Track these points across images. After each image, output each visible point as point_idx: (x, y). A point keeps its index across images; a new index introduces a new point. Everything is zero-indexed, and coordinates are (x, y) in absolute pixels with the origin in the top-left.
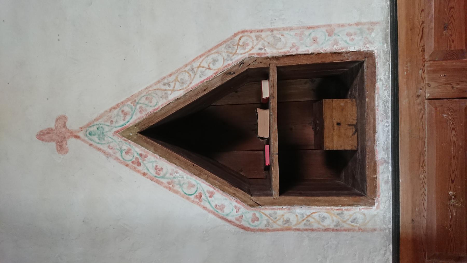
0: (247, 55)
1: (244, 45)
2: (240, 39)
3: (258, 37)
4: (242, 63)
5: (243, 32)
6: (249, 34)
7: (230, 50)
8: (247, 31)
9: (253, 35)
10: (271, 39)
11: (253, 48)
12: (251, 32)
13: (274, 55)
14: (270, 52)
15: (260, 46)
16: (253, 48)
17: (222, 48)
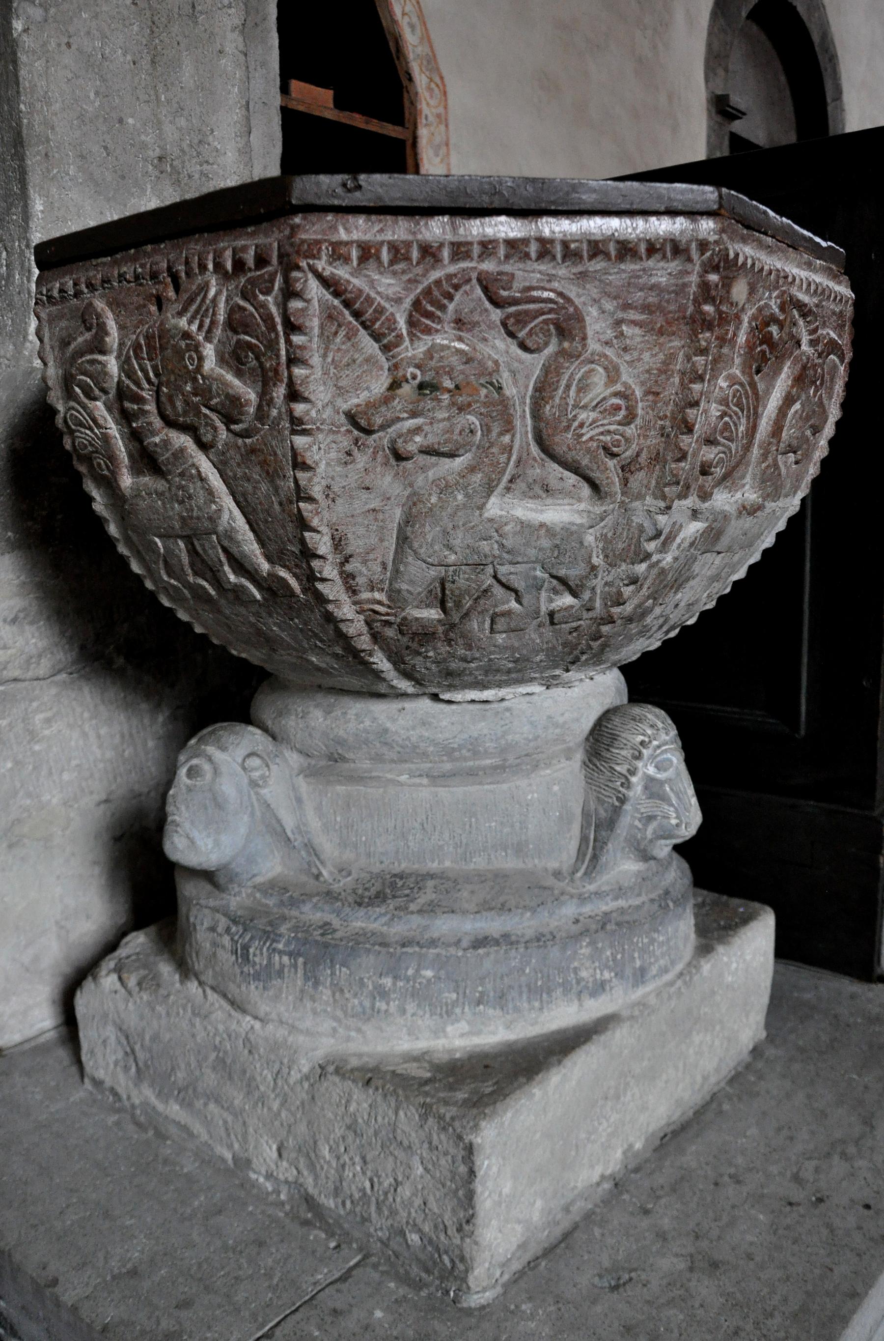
0: (420, 90)
1: (430, 89)
2: (437, 86)
3: (439, 116)
4: (410, 79)
5: (445, 93)
6: (443, 104)
7: (425, 63)
8: (446, 100)
9: (441, 110)
10: (438, 139)
11: (428, 104)
12: (446, 108)
13: (419, 140)
14: (423, 133)
15: (431, 118)
16: (428, 104)
17: (427, 50)
